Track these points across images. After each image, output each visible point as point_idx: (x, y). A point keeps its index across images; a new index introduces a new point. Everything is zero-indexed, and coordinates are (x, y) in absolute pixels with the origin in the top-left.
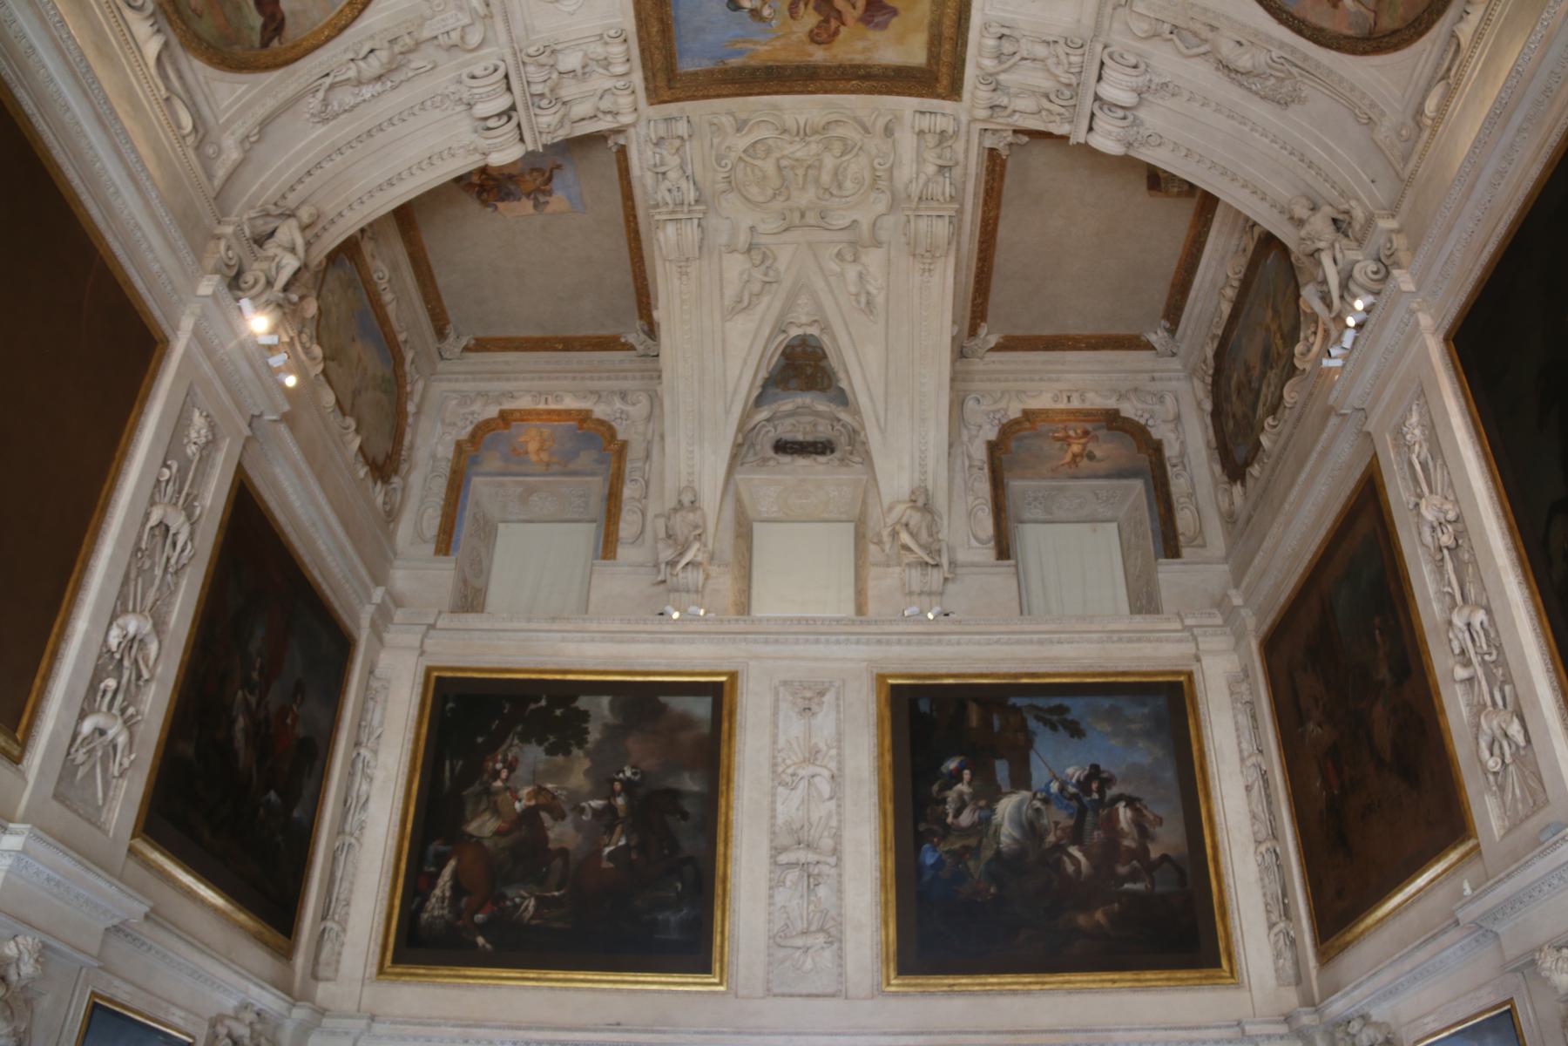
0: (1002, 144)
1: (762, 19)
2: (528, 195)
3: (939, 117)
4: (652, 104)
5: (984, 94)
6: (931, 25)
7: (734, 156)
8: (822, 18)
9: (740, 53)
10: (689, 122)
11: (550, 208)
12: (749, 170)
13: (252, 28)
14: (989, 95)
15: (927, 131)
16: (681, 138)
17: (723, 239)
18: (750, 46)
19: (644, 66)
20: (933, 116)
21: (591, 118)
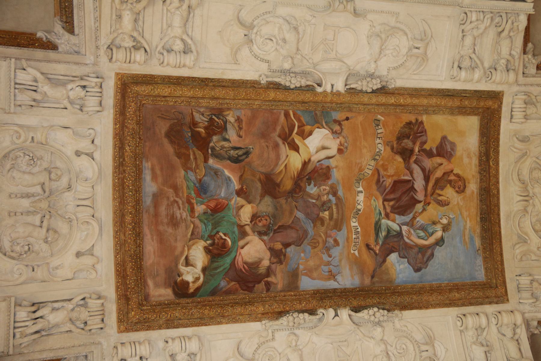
0: (534, 61)
1: (449, 224)
3: (514, 106)
4: (508, 300)
5: (498, 76)
6: (452, 114)
8: (448, 185)
9: (472, 239)
10: (520, 275)
14: (499, 72)
15: (524, 113)
16: (532, 281)
18: (467, 232)
19: (481, 304)
20: (514, 110)
21: (518, 344)
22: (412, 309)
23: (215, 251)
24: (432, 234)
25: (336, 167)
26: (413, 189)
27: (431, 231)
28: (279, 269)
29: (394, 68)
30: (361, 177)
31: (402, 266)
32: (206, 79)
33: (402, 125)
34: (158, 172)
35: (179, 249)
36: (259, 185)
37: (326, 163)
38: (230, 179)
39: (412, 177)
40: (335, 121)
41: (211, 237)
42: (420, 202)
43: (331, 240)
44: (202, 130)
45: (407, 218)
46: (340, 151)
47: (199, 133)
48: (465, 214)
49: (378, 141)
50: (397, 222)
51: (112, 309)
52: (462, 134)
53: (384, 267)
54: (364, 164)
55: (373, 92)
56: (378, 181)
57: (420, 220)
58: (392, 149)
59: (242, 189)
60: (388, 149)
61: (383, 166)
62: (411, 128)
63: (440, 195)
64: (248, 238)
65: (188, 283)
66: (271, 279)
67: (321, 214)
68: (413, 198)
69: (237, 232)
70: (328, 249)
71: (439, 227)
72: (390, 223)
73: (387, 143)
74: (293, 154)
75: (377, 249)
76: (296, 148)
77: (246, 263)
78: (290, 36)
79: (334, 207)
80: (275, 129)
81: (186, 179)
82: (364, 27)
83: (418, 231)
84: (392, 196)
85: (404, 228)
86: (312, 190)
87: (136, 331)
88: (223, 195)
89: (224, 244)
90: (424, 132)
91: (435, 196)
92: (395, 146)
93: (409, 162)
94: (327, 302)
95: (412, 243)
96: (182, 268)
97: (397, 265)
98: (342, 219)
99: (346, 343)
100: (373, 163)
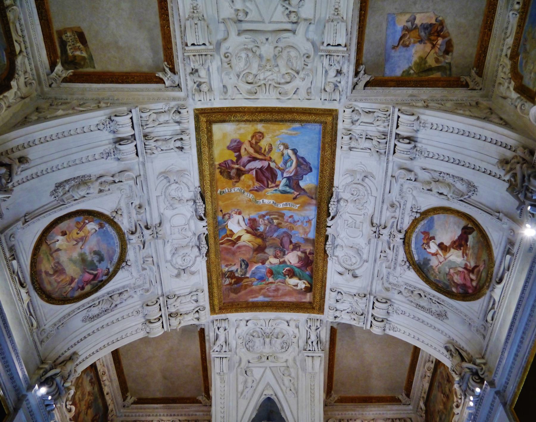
0: (169, 75)
1: (284, 144)
2: (416, 27)
4: (336, 110)
7: (302, 75)
11: (407, 17)
12: (295, 66)
13: (474, 238)
15: (207, 93)
17: (312, 27)
18: (290, 132)
22: (333, 179)
23: (292, 274)
24: (290, 157)
25: (249, 215)
26: (261, 169)
27: (287, 157)
28: (303, 248)
29: (189, 188)
30: (254, 200)
31: (308, 179)
32: (208, 282)
33: (222, 177)
34: (254, 296)
35: (290, 288)
36: (259, 255)
37: (247, 221)
38: (256, 268)
39: (253, 169)
40: (223, 218)
41: (285, 275)
42: (269, 164)
43: (290, 220)
44: (233, 281)
45: (279, 173)
46: (240, 213)
47: (234, 282)
48: (277, 133)
49: (233, 191)
50: (281, 179)
51: (313, 316)
52: (225, 136)
53: (308, 191)
54: (247, 199)
55: (204, 203)
56: (256, 190)
57: (280, 164)
58: (237, 182)
59: (261, 262)
60: (237, 184)
61: (247, 188)
62: (224, 172)
63: (265, 150)
64: (286, 260)
65: (306, 287)
66: (308, 251)
67: (275, 224)
68: (267, 169)
69: (283, 265)
70: (295, 222)
71: (285, 152)
72: (282, 184)
73: (234, 186)
74: (243, 239)
75: (296, 193)
76: (239, 237)
77: (298, 262)
78: (182, 252)
79: (271, 217)
80: (230, 249)
81: (257, 285)
82: (168, 213)
83: (287, 166)
84: (266, 182)
85: (285, 175)
86: (262, 228)
87: (324, 309)
88: (264, 270)
89: (289, 270)
90: (225, 162)
91: (265, 153)
92: (235, 180)
93: (244, 171)
94: (323, 231)
95: (294, 171)
96: (299, 288)
97: (307, 182)
98: (278, 213)
99: (346, 222)
100: (246, 194)
